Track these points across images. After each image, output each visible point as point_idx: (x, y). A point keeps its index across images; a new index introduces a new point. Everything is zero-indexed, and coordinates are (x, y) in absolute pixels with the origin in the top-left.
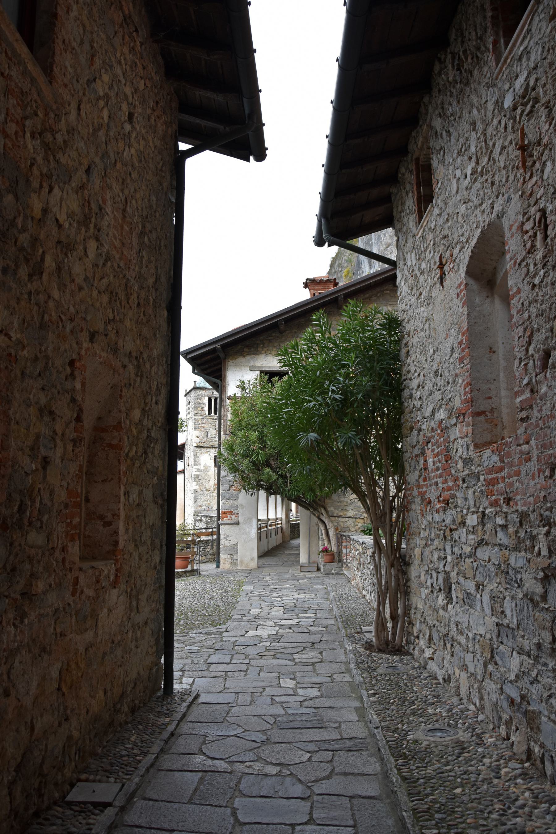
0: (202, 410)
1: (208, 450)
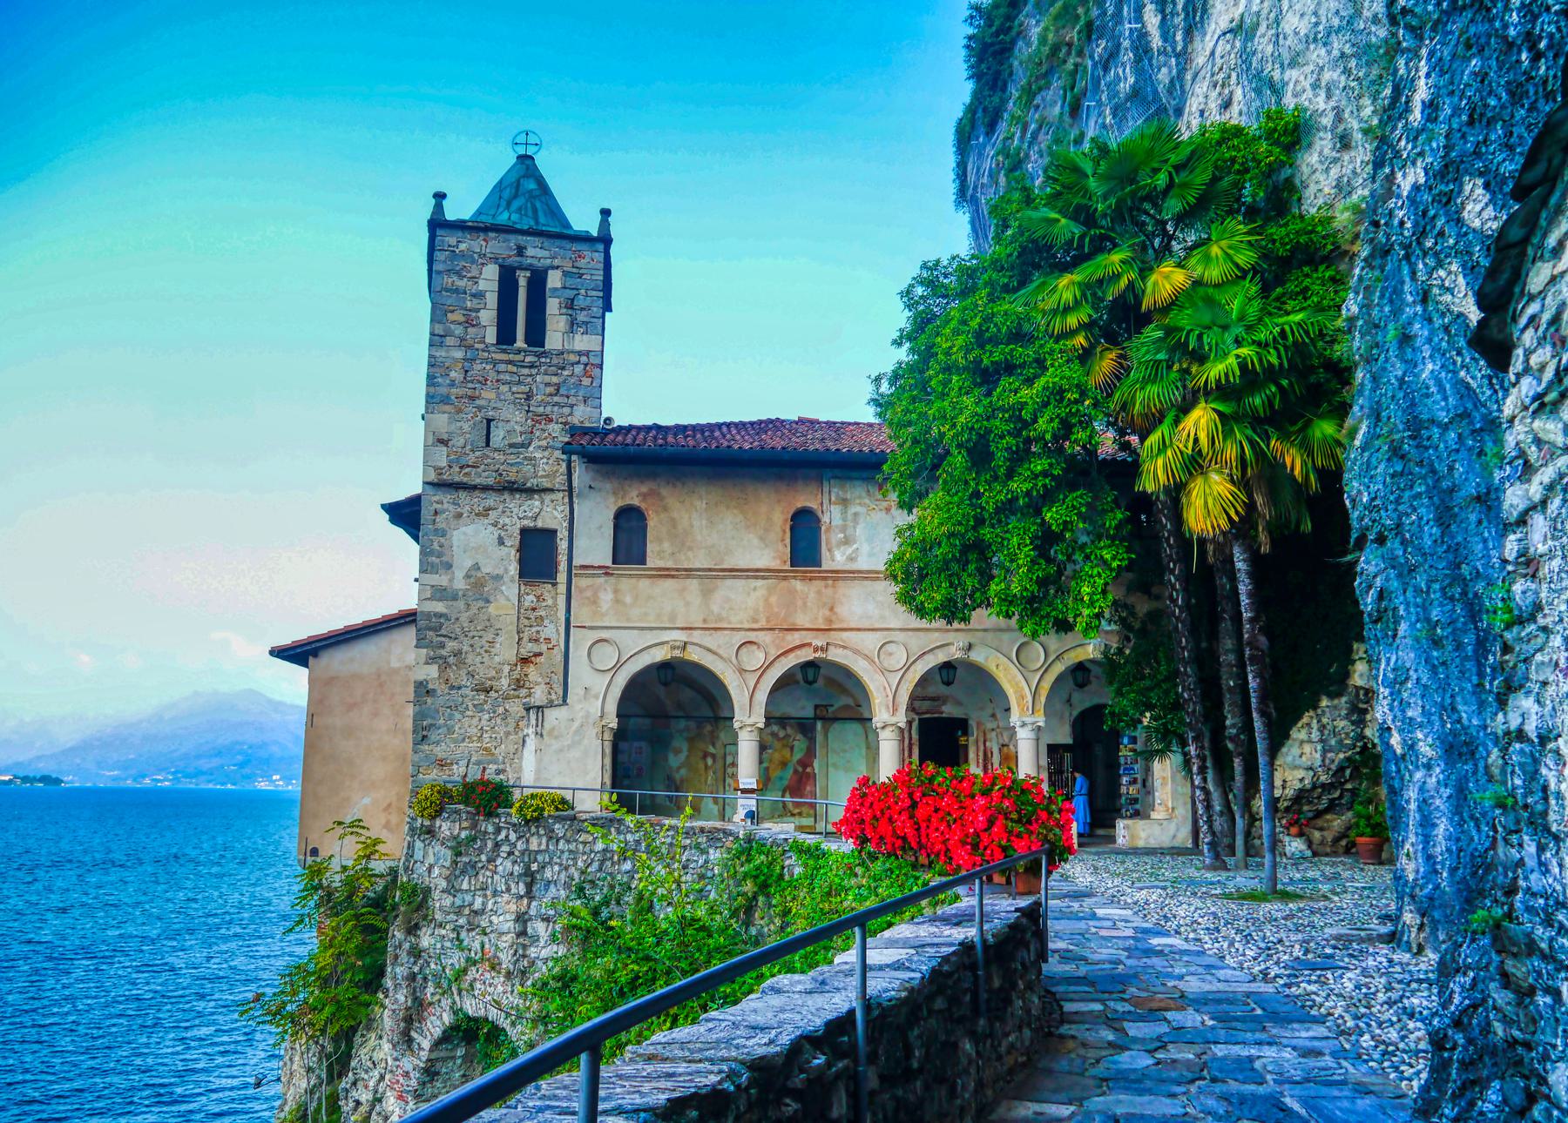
0: (470, 322)
1: (491, 500)
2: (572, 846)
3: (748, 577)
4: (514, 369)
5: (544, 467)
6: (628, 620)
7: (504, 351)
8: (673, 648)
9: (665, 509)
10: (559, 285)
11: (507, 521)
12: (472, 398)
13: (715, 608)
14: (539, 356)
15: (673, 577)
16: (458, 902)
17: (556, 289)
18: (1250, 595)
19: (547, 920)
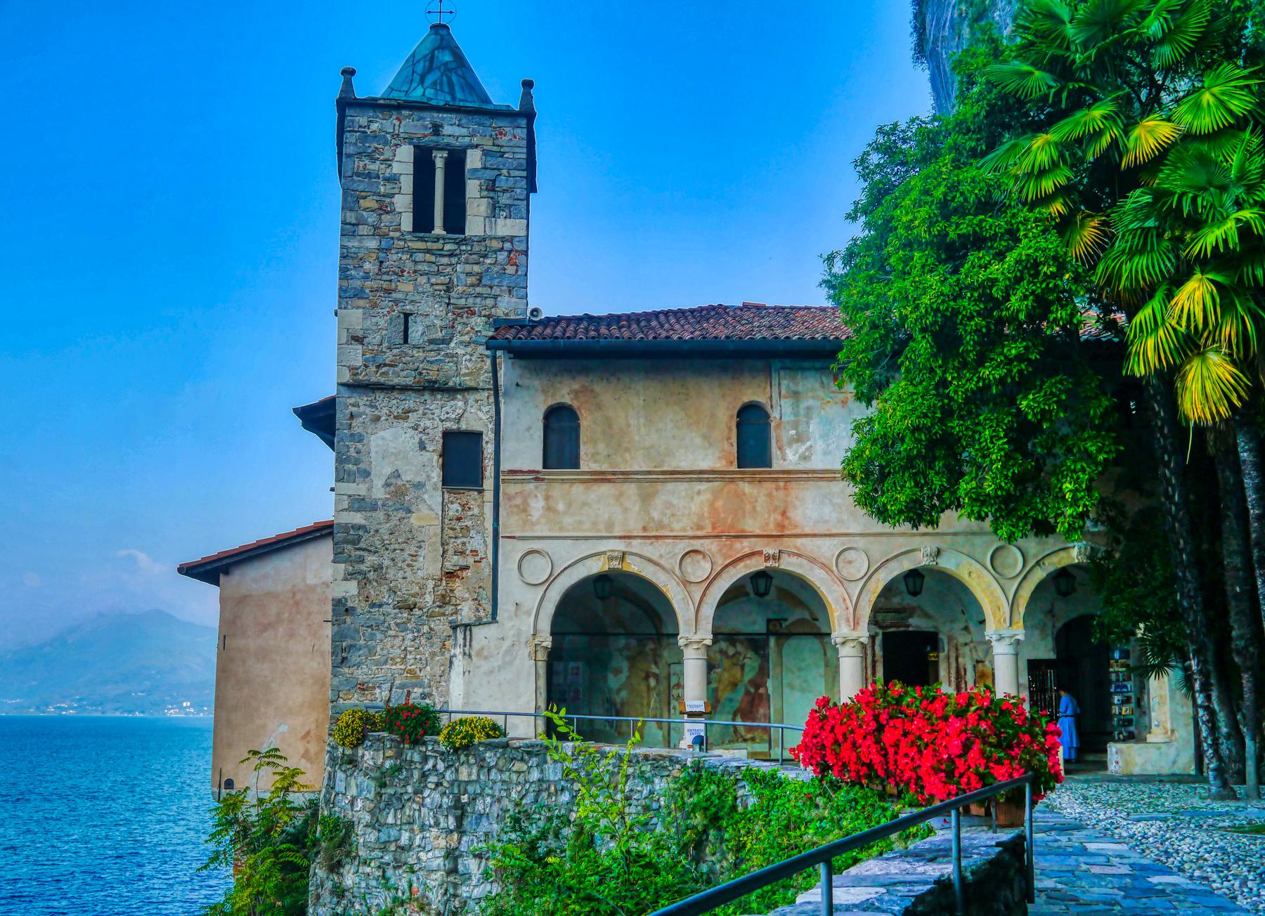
0: (384, 208)
1: (411, 401)
2: (505, 776)
3: (691, 480)
4: (433, 259)
5: (466, 365)
6: (561, 529)
7: (422, 239)
8: (611, 559)
9: (599, 407)
10: (479, 165)
11: (429, 424)
12: (388, 292)
13: (656, 515)
14: (459, 243)
15: (609, 481)
16: (384, 837)
17: (476, 170)
18: (1257, 489)
19: (479, 856)
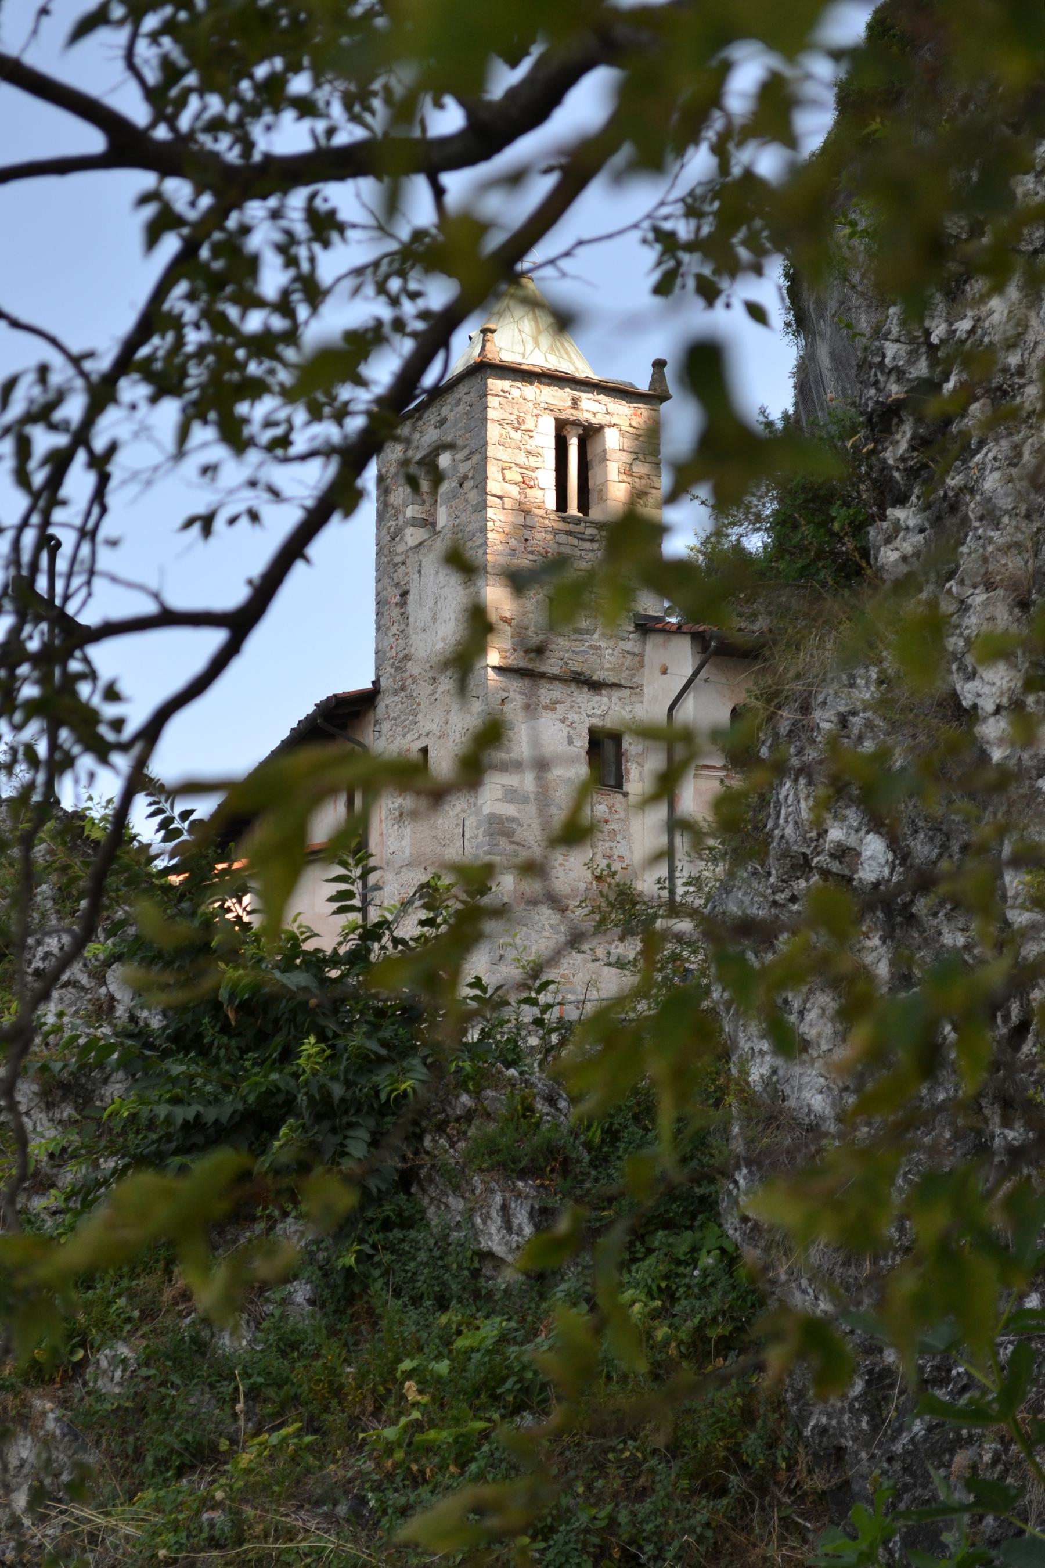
4: (575, 542)
